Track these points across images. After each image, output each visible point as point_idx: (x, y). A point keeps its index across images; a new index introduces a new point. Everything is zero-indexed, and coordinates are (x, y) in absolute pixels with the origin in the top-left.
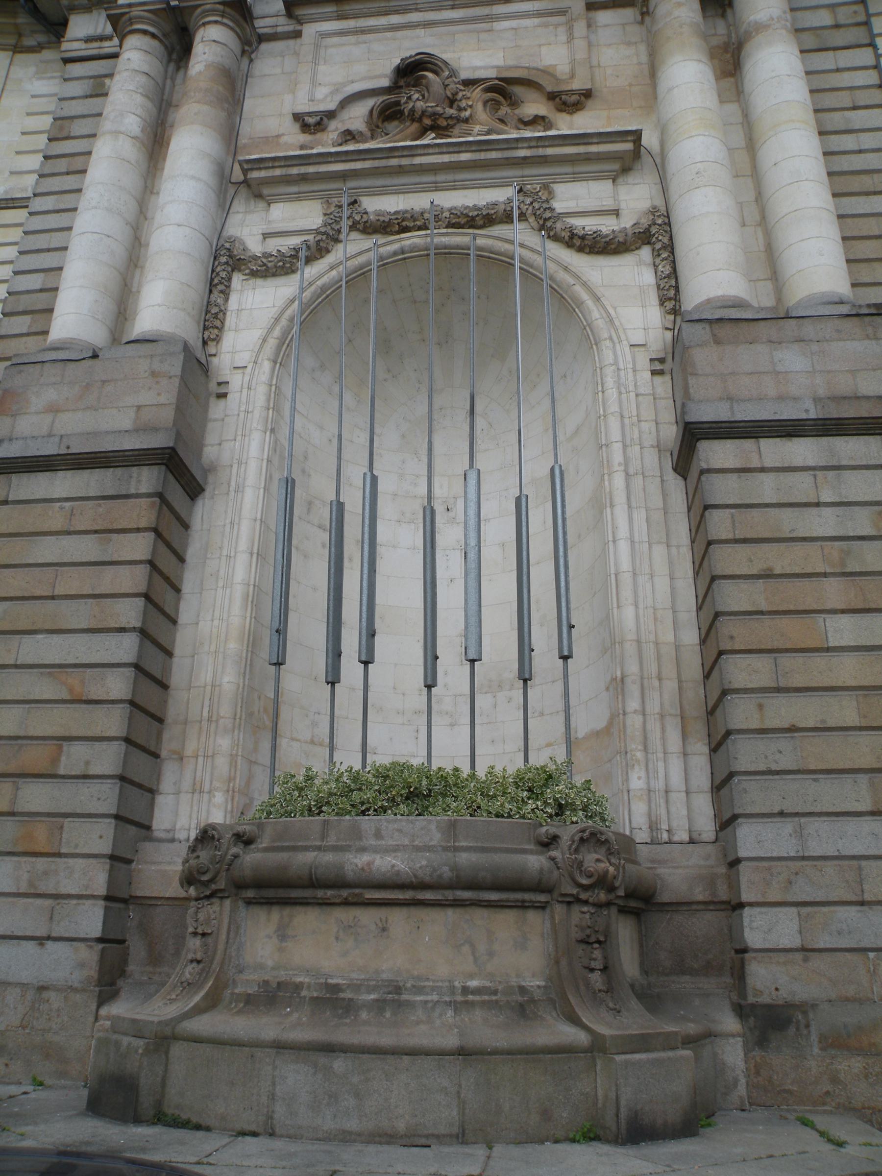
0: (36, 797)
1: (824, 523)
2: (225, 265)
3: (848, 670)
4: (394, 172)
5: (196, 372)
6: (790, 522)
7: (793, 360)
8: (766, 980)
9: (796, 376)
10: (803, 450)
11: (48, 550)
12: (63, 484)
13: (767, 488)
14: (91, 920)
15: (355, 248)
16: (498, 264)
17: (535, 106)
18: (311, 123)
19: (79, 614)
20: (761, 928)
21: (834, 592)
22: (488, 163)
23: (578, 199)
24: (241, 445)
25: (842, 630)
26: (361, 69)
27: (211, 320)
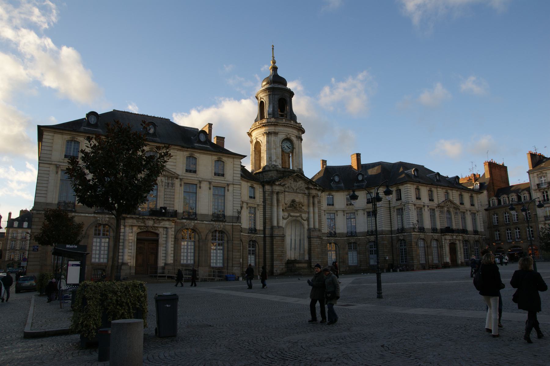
0: (281, 258)
4: (293, 211)
12: (279, 238)
15: (290, 218)
16: (298, 221)
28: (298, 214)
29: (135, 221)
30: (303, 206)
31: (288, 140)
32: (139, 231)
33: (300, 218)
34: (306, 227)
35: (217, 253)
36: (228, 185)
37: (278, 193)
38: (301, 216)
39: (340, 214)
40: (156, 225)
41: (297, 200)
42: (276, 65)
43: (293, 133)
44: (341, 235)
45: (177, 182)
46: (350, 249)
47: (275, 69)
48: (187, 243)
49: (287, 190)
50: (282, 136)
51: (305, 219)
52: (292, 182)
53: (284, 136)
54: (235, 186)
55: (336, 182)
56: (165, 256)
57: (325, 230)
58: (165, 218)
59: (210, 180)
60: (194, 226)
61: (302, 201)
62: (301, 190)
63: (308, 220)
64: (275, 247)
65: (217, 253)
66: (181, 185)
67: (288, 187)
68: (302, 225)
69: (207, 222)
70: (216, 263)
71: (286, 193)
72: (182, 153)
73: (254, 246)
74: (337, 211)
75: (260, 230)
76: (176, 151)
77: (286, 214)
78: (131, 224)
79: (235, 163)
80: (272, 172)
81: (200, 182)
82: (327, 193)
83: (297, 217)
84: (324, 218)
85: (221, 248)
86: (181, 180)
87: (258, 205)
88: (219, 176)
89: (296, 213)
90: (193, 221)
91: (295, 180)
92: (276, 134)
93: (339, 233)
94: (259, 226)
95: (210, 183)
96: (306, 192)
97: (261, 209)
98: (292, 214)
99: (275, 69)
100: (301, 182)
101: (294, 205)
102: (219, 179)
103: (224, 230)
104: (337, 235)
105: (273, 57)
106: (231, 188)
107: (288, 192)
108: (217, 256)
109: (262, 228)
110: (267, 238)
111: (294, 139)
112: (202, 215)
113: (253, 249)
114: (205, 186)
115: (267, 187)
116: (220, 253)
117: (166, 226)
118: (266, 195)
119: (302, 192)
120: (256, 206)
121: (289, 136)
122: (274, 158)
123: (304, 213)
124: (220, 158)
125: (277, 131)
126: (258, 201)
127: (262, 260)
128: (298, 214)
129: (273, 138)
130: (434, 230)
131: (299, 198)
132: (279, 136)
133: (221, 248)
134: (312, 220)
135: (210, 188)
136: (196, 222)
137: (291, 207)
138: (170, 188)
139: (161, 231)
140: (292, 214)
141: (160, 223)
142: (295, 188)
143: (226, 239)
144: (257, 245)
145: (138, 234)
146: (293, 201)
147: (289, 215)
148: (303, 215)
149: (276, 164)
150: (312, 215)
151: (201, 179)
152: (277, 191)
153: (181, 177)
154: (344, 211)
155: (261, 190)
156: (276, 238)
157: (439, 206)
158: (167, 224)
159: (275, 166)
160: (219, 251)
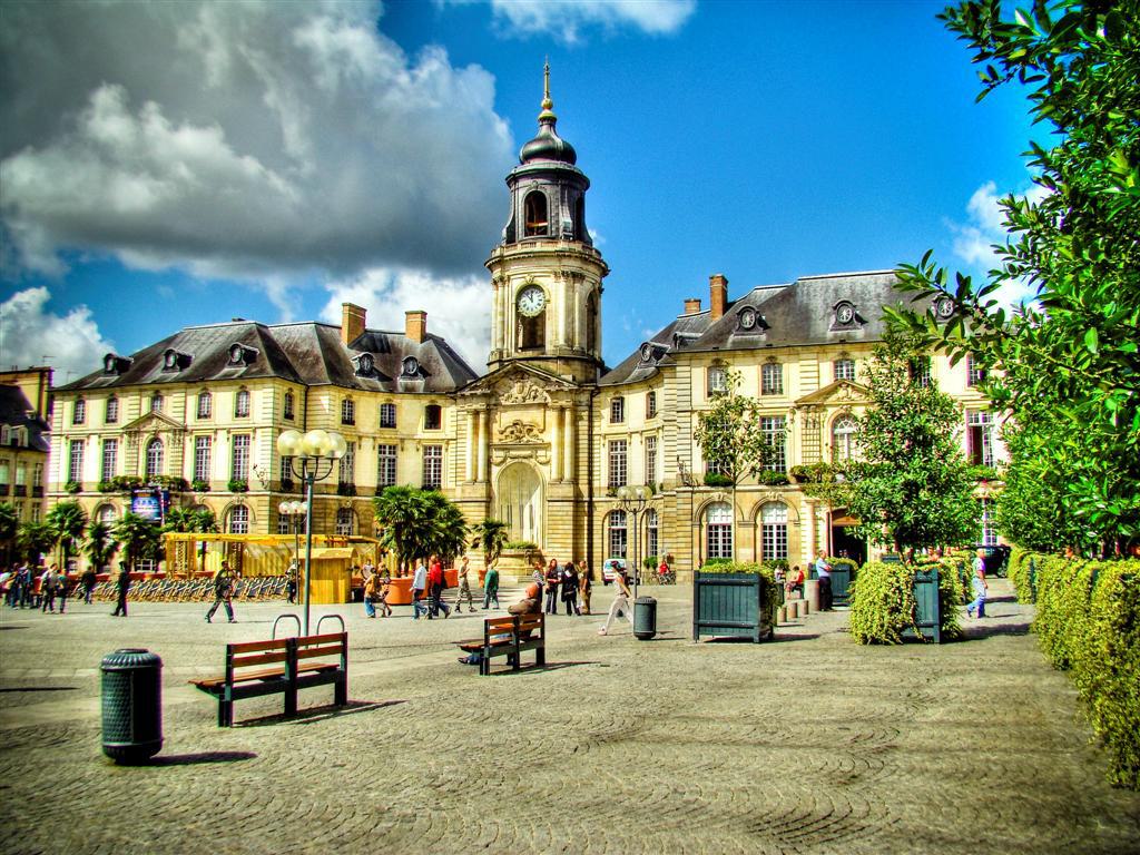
2: (489, 464)
7: (560, 491)
28: (528, 453)
30: (542, 432)
37: (476, 413)
51: (543, 459)
61: (539, 420)
62: (534, 398)
83: (525, 458)
89: (523, 449)
102: (242, 422)
111: (547, 282)
114: (222, 435)
128: (528, 453)
140: (513, 453)
143: (250, 517)
146: (515, 424)
154: (641, 433)
157: (801, 405)
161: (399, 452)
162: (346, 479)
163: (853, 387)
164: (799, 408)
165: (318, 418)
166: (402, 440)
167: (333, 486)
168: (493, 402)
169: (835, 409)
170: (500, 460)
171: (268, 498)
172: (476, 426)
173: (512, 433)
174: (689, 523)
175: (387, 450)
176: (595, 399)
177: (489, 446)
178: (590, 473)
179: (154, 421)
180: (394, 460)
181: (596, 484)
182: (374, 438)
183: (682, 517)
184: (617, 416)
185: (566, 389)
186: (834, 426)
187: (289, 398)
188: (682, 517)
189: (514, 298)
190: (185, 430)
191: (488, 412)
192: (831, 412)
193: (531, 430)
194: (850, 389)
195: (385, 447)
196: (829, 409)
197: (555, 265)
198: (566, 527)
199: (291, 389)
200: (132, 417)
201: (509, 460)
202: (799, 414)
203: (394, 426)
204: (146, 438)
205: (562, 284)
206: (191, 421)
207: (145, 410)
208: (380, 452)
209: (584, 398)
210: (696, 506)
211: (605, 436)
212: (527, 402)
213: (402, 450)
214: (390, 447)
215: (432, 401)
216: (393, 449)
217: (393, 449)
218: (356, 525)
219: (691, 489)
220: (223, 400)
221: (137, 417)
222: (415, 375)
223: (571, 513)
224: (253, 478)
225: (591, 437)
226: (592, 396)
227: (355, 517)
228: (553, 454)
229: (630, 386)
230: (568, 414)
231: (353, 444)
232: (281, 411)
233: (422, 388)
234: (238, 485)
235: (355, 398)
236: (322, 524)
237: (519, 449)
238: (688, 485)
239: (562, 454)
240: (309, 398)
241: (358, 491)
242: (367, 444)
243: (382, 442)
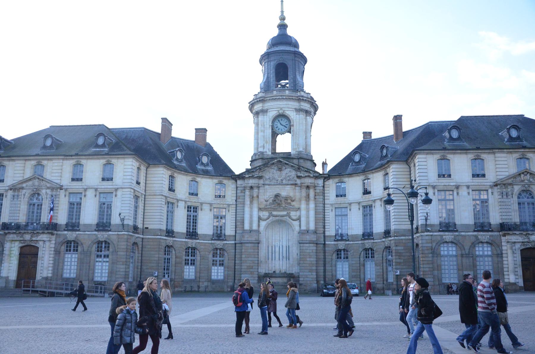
0: (251, 270)
1: (308, 251)
2: (260, 219)
3: (308, 262)
4: (275, 210)
5: (258, 231)
6: (306, 251)
7: (308, 237)
8: (301, 282)
9: (308, 237)
10: (307, 245)
11: (250, 251)
12: (250, 245)
13: (304, 248)
14: (257, 279)
17: (289, 201)
18: (266, 201)
19: (253, 256)
20: (301, 279)
21: (308, 256)
22: (285, 209)
23: (293, 214)
24: (263, 240)
25: (308, 259)
26: (271, 194)
27: (259, 226)
28: (285, 213)
29: (15, 235)
30: (293, 201)
31: (281, 116)
32: (21, 245)
33: (287, 218)
34: (297, 228)
35: (102, 266)
36: (116, 190)
37: (252, 188)
38: (288, 215)
39: (355, 208)
40: (34, 239)
41: (284, 194)
42: (286, 22)
43: (289, 108)
44: (355, 238)
45: (62, 193)
46: (339, 257)
47: (283, 27)
48: (72, 256)
49: (267, 182)
50: (272, 114)
52: (275, 171)
53: (275, 112)
54: (124, 190)
55: (356, 162)
56: (44, 268)
57: (331, 231)
58: (41, 232)
59: (96, 187)
60: (76, 237)
61: (291, 194)
62: (289, 180)
63: (299, 219)
64: (243, 256)
65: (102, 266)
66: (65, 195)
67: (269, 179)
68: (289, 226)
69: (89, 233)
70: (101, 277)
71: (267, 187)
72: (68, 162)
73: (222, 255)
74: (350, 204)
75: (230, 236)
76: (61, 161)
77: (265, 214)
78: (11, 239)
79: (126, 163)
80: (258, 161)
81: (85, 190)
82: (337, 180)
84: (330, 215)
85: (108, 260)
86: (66, 190)
87: (229, 205)
88: (108, 180)
89: (281, 211)
90: (74, 233)
91: (280, 170)
92: (264, 112)
93: (352, 235)
94: (229, 231)
95: (96, 190)
96: (299, 181)
97: (232, 210)
98: (275, 213)
99: (283, 27)
100: (288, 170)
101: (278, 201)
102: (107, 185)
103: (108, 241)
104: (350, 238)
105: (282, 12)
106: (119, 193)
107: (269, 185)
108: (102, 269)
109: (233, 233)
110: (237, 245)
111: (292, 114)
112: (85, 225)
113: (221, 259)
114: (90, 193)
115: (239, 182)
116: (106, 266)
117: (44, 239)
118: (238, 191)
119: (292, 182)
120: (225, 206)
121: (281, 112)
122: (261, 143)
123: (293, 211)
124: (108, 161)
125: (265, 108)
126: (230, 200)
127: (232, 273)
128: (285, 213)
129: (261, 117)
130: (482, 227)
131: (286, 191)
132: (268, 114)
133: (108, 260)
134: (303, 219)
135: (96, 196)
136: (77, 233)
137: (274, 204)
138: (15, 200)
139: (40, 245)
140: (275, 213)
141: (37, 236)
142: (280, 179)
143: (111, 250)
144: (226, 254)
145: (21, 248)
146: (277, 196)
147: (271, 215)
148: (293, 214)
149: (265, 150)
150: (303, 212)
151: (85, 187)
152: (250, 185)
153: (66, 187)
154: (359, 203)
155: (234, 186)
156: (247, 245)
158: (44, 237)
159: (262, 153)
160: (104, 264)
161: (199, 212)
162: (169, 228)
163: (531, 174)
164: (496, 185)
165: (155, 185)
166: (202, 204)
167: (163, 230)
168: (261, 182)
169: (520, 186)
170: (265, 217)
171: (126, 237)
172: (252, 198)
173: (275, 201)
174: (430, 255)
175: (192, 209)
176: (326, 183)
177: (260, 209)
178: (324, 227)
179: (36, 182)
180: (196, 216)
181: (327, 234)
182: (186, 202)
183: (426, 252)
184: (341, 195)
185: (312, 175)
186: (519, 198)
187: (139, 168)
188: (426, 252)
189: (271, 122)
190: (61, 189)
191: (258, 187)
192: (517, 189)
193: (287, 200)
194: (528, 175)
195: (191, 208)
196: (515, 186)
197: (295, 104)
198: (312, 259)
199: (140, 165)
200: (15, 179)
201: (271, 218)
202: (496, 190)
203: (197, 195)
204: (27, 193)
205: (302, 116)
206: (66, 181)
207: (28, 174)
208: (188, 211)
209: (320, 182)
210: (434, 244)
211: (332, 205)
212: (284, 182)
213: (201, 209)
214: (194, 208)
215: (221, 181)
216: (195, 209)
217: (195, 209)
218: (174, 257)
219: (431, 234)
220: (93, 169)
221: (21, 179)
222: (208, 165)
223: (314, 251)
224: (115, 220)
225: (324, 204)
226: (324, 182)
227: (174, 252)
228: (303, 212)
229: (350, 175)
230: (312, 193)
231: (173, 204)
232: (135, 179)
233: (213, 171)
234: (103, 225)
235: (176, 175)
236: (157, 256)
237: (279, 211)
238: (428, 231)
239: (308, 217)
240: (148, 172)
241: (175, 235)
242: (182, 205)
243: (189, 204)
